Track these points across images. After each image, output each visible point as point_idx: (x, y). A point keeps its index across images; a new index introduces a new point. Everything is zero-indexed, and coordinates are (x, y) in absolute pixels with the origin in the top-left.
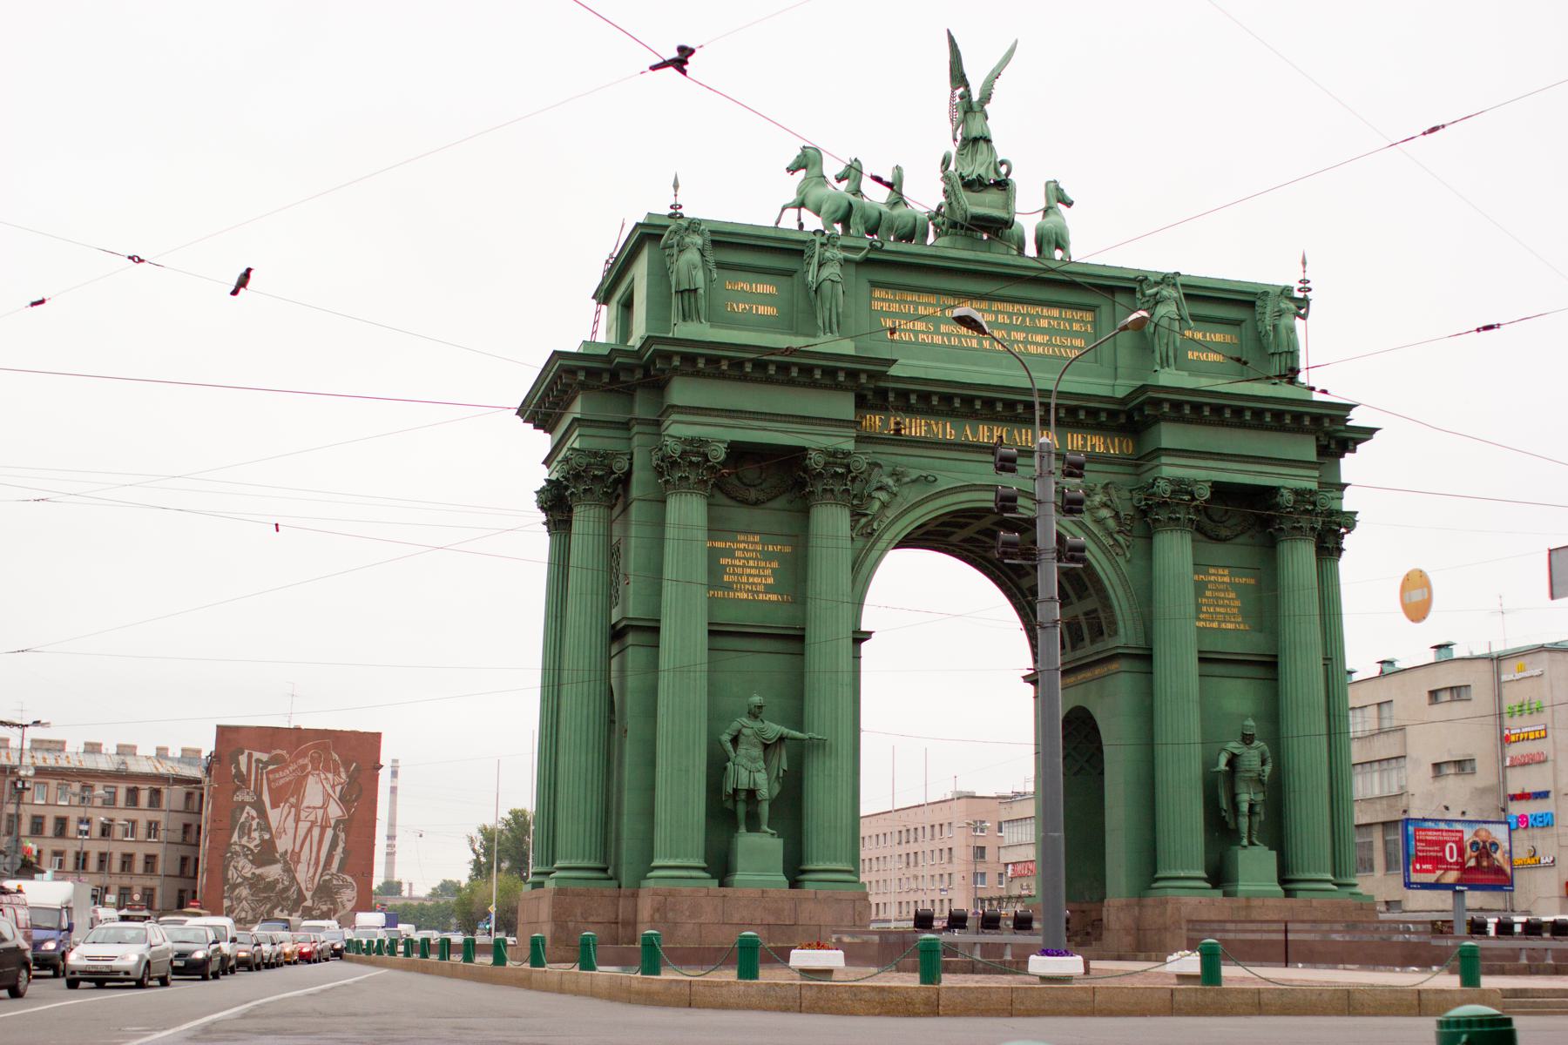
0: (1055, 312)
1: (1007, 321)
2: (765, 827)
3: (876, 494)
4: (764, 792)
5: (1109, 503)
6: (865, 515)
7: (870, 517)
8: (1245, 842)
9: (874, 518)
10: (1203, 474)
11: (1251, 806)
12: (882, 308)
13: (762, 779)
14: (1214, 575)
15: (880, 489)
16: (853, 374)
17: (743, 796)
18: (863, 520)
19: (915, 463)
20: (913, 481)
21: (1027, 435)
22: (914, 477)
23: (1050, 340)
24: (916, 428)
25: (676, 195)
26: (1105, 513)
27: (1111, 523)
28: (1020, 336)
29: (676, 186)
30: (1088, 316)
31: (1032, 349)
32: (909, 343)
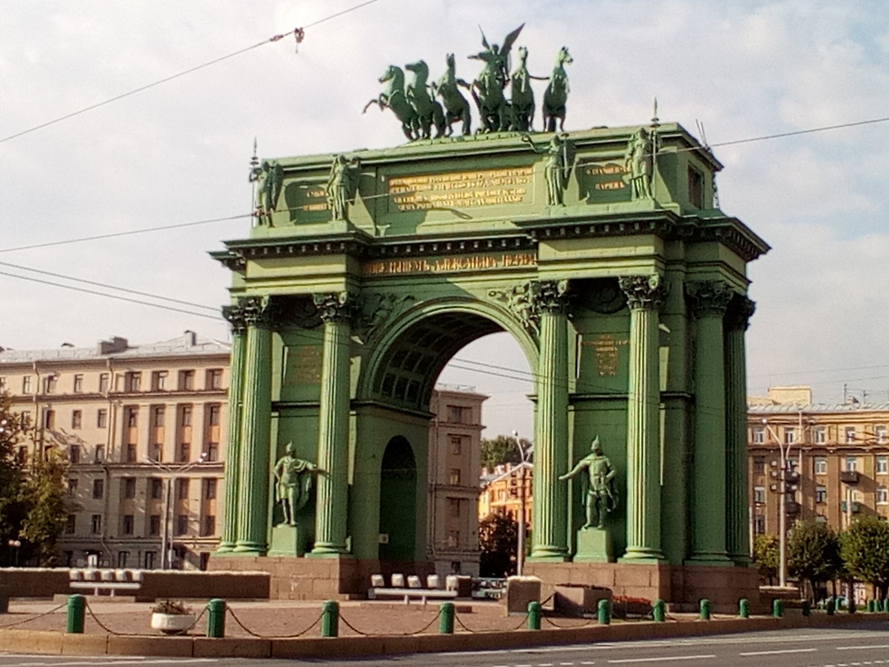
0: (504, 173)
1: (473, 185)
2: (293, 523)
3: (378, 313)
4: (291, 502)
5: (526, 299)
6: (372, 327)
7: (374, 328)
8: (587, 525)
9: (379, 326)
10: (562, 275)
11: (597, 500)
12: (395, 191)
13: (291, 492)
14: (604, 340)
15: (380, 309)
16: (335, 245)
17: (284, 502)
18: (372, 330)
19: (402, 291)
20: (405, 300)
21: (475, 259)
22: (403, 299)
23: (501, 192)
24: (405, 267)
25: (255, 151)
26: (522, 306)
27: (524, 312)
28: (482, 194)
29: (255, 147)
30: (529, 171)
31: (489, 201)
32: (411, 210)
